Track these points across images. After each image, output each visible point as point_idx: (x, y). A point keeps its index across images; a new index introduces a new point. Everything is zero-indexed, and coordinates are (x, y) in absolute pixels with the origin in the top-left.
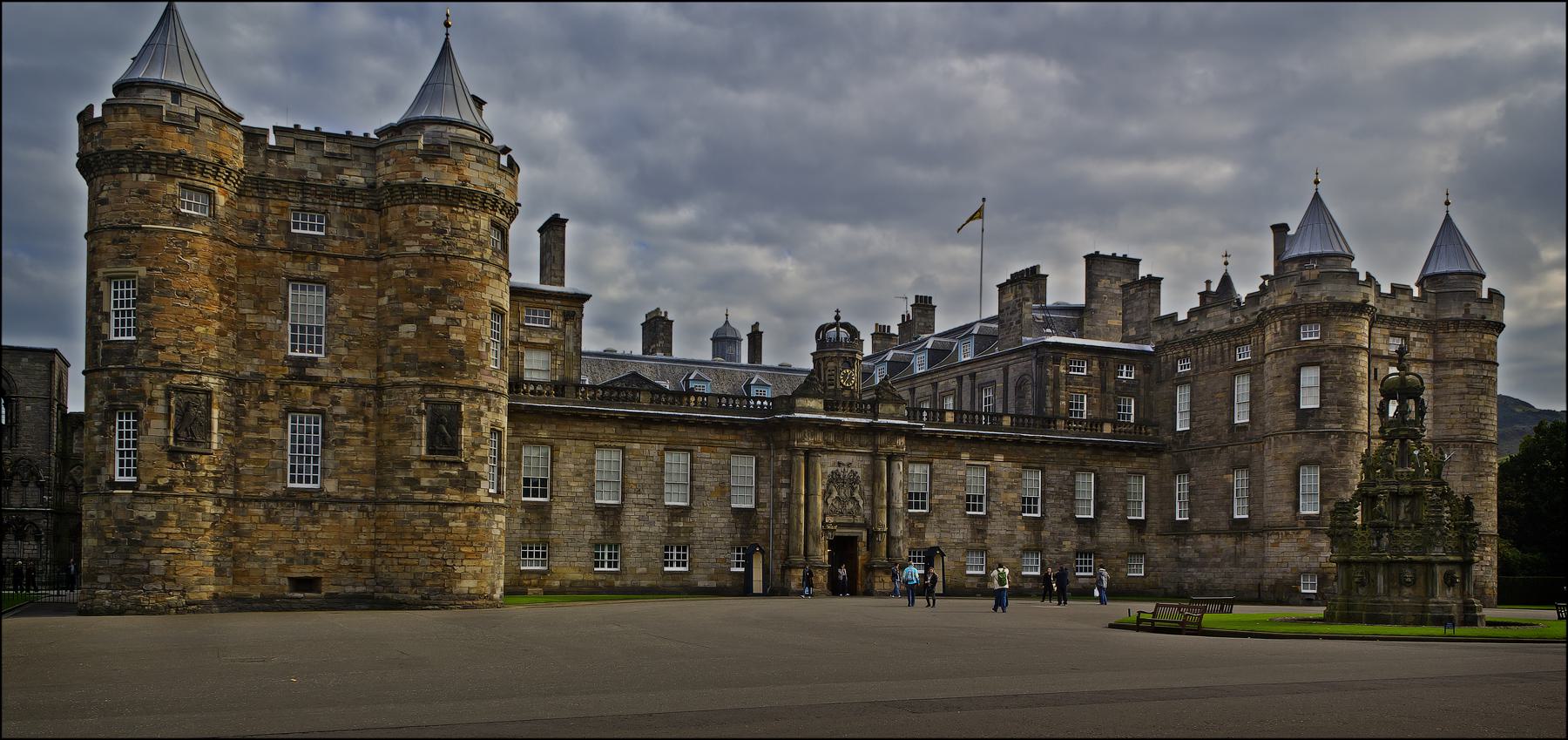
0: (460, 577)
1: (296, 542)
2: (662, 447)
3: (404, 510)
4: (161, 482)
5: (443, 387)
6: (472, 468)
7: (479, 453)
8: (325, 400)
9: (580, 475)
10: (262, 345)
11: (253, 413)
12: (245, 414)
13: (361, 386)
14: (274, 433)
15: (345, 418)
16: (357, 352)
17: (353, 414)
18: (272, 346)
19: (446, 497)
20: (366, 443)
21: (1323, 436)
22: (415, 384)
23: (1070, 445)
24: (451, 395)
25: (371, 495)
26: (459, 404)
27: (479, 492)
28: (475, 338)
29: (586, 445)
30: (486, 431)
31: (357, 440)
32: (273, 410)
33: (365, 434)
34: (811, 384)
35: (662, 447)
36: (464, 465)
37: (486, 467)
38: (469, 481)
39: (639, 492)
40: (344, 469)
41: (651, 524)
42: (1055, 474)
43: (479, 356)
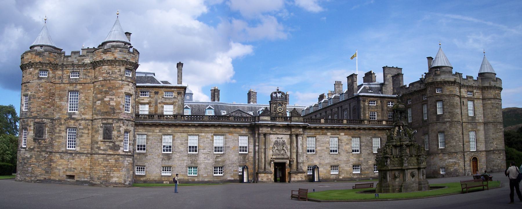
0: (112, 177)
1: (68, 165)
2: (212, 134)
3: (96, 156)
4: (31, 147)
5: (107, 119)
6: (117, 143)
7: (120, 139)
8: (77, 124)
9: (183, 144)
10: (61, 110)
11: (58, 129)
12: (56, 129)
13: (87, 120)
14: (63, 134)
15: (82, 129)
16: (87, 110)
17: (85, 128)
18: (63, 110)
19: (108, 152)
20: (88, 136)
21: (445, 123)
22: (100, 119)
23: (369, 129)
24: (110, 121)
25: (89, 152)
26: (112, 124)
27: (119, 151)
28: (118, 104)
29: (185, 135)
30: (122, 132)
31: (86, 135)
32: (63, 128)
33: (88, 134)
34: (266, 112)
35: (212, 134)
36: (114, 143)
37: (122, 143)
38: (116, 148)
39: (204, 149)
40: (82, 144)
41: (209, 160)
42: (364, 139)
43: (120, 109)
